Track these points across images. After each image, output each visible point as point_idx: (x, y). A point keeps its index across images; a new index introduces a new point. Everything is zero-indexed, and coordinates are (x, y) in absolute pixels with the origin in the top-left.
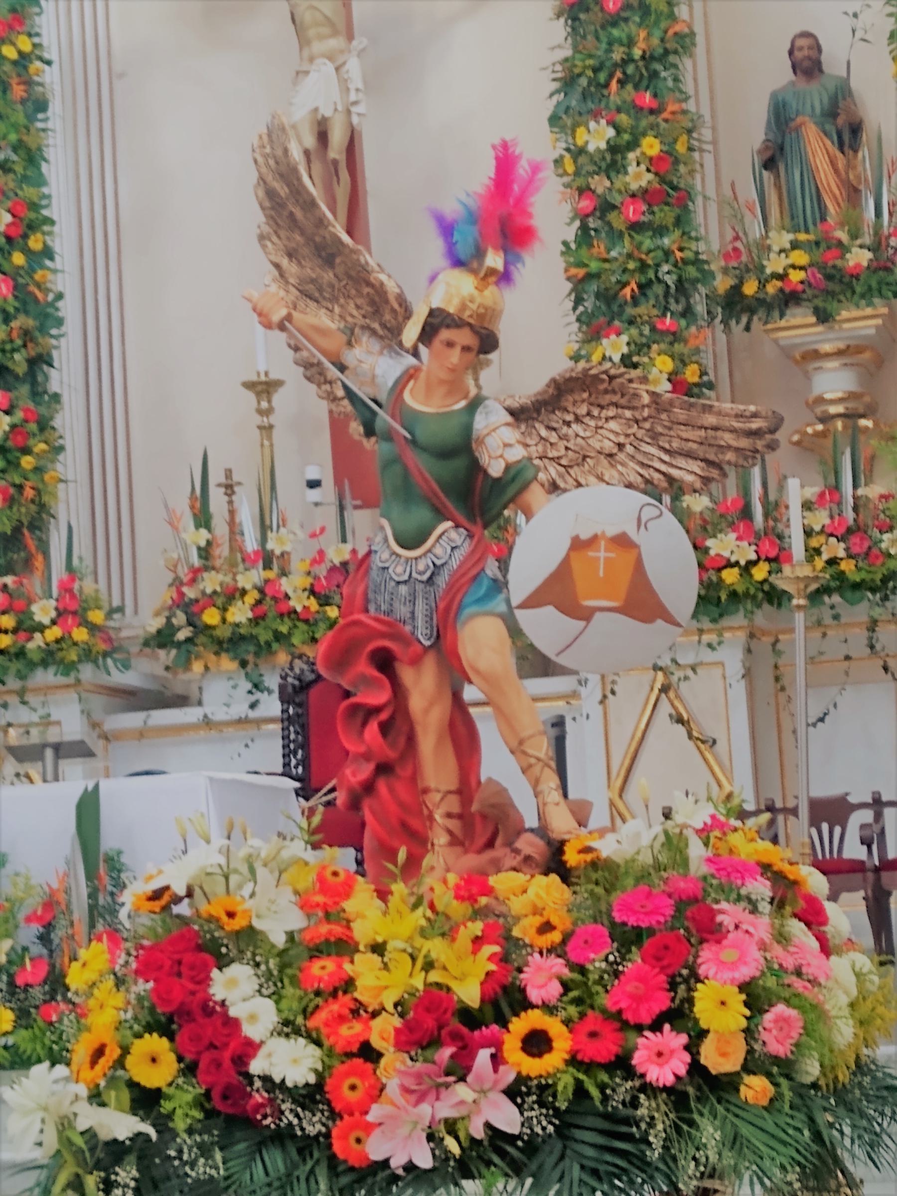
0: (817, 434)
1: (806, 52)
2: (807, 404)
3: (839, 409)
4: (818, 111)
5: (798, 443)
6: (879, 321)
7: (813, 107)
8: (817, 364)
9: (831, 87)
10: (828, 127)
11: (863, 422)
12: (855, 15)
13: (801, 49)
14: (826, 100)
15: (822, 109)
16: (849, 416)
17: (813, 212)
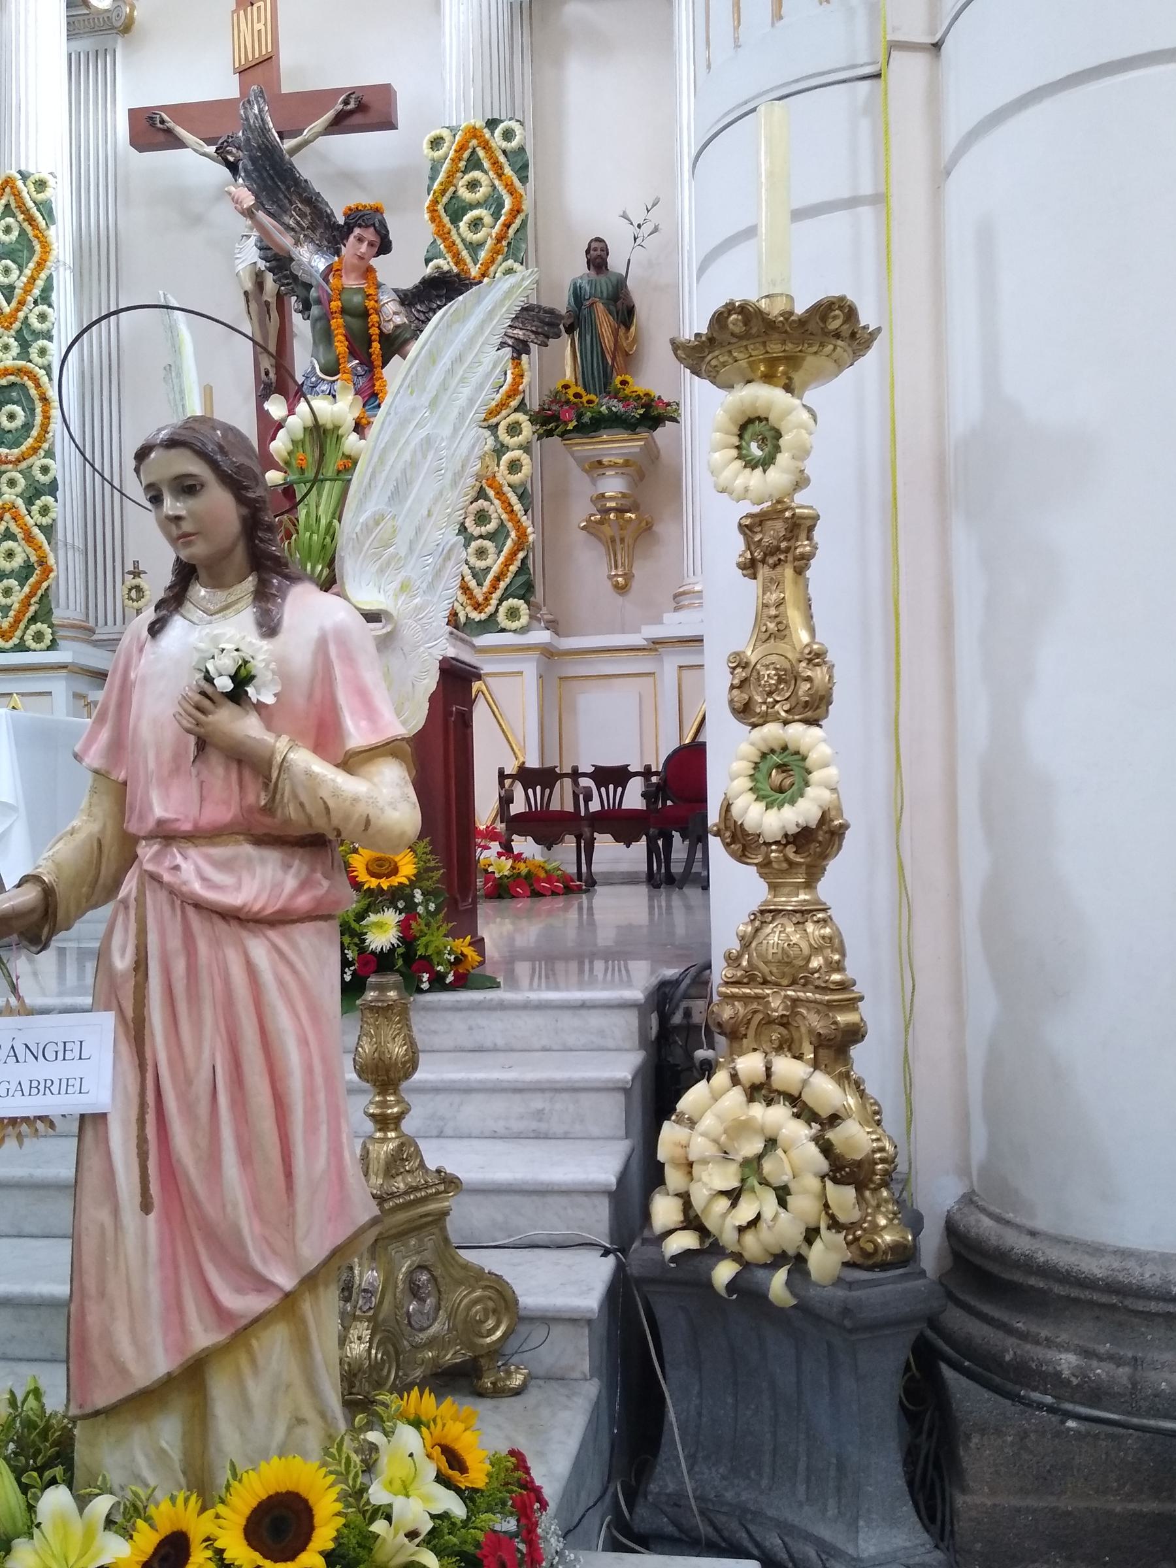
0: (596, 522)
1: (599, 252)
2: (591, 500)
3: (613, 504)
4: (605, 295)
5: (584, 528)
6: (642, 443)
7: (602, 292)
8: (601, 471)
9: (614, 279)
10: (612, 307)
11: (629, 514)
12: (639, 226)
13: (595, 250)
14: (610, 288)
15: (608, 294)
16: (620, 511)
17: (598, 363)
